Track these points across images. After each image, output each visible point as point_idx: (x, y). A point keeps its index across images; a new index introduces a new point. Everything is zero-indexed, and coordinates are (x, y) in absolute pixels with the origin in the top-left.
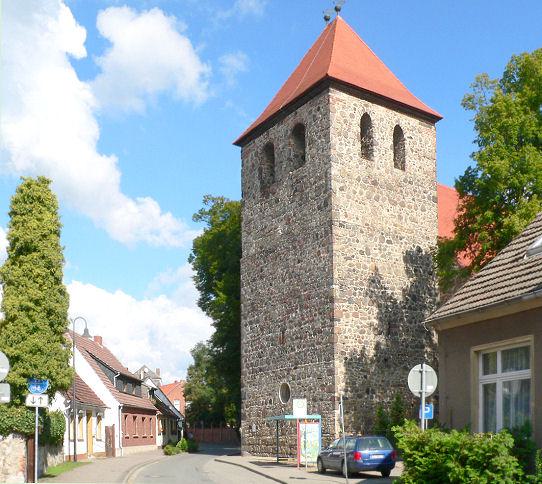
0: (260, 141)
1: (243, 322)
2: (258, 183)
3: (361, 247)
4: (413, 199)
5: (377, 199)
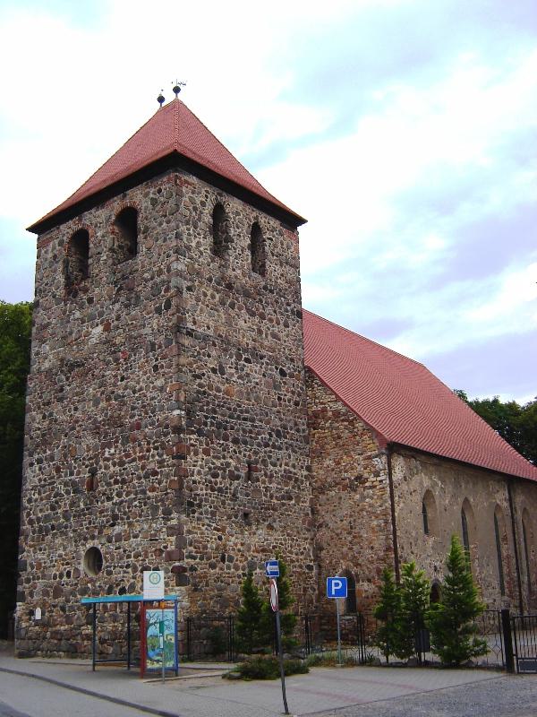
0: (68, 229)
1: (27, 460)
2: (61, 278)
3: (212, 364)
4: (275, 312)
5: (232, 306)
